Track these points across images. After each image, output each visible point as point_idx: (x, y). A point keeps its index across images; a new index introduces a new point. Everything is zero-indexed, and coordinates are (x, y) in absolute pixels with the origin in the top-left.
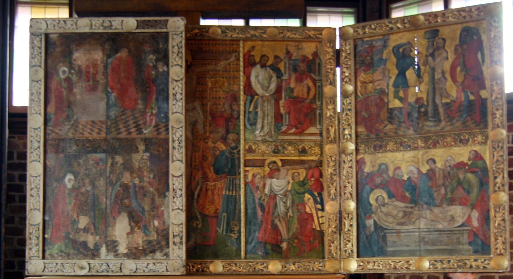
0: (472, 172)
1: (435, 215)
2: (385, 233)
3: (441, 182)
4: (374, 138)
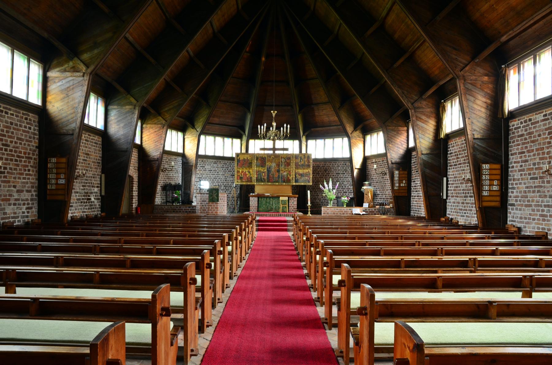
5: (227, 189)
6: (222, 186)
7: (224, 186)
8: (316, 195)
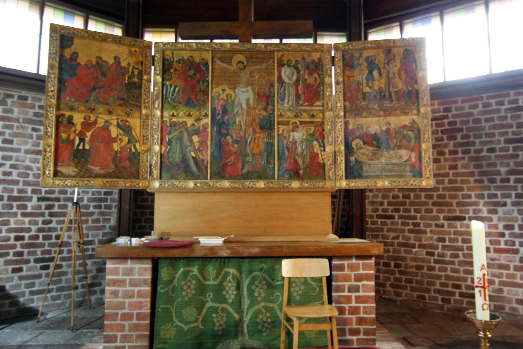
0: (411, 131)
3: (393, 136)
5: (56, 210)
6: (30, 199)
7: (40, 199)
8: (410, 231)
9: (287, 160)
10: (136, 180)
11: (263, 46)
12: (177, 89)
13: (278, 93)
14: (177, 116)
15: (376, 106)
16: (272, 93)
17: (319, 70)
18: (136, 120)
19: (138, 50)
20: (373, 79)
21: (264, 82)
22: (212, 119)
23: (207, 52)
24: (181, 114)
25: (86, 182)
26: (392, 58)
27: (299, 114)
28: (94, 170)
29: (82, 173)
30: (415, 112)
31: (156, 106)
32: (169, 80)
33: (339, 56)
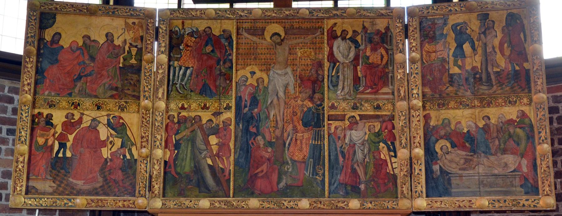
0: (520, 128)
1: (491, 162)
2: (450, 177)
3: (495, 135)
4: (438, 98)
9: (342, 170)
10: (130, 198)
11: (308, 12)
12: (188, 72)
13: (328, 76)
14: (189, 109)
15: (469, 93)
16: (321, 76)
17: (387, 44)
18: (132, 115)
19: (136, 21)
20: (463, 56)
21: (309, 62)
22: (236, 113)
23: (231, 21)
24: (194, 105)
25: (65, 201)
26: (491, 26)
27: (358, 105)
28: (76, 185)
29: (61, 189)
30: (525, 100)
31: (160, 95)
32: (178, 59)
33: (415, 23)
